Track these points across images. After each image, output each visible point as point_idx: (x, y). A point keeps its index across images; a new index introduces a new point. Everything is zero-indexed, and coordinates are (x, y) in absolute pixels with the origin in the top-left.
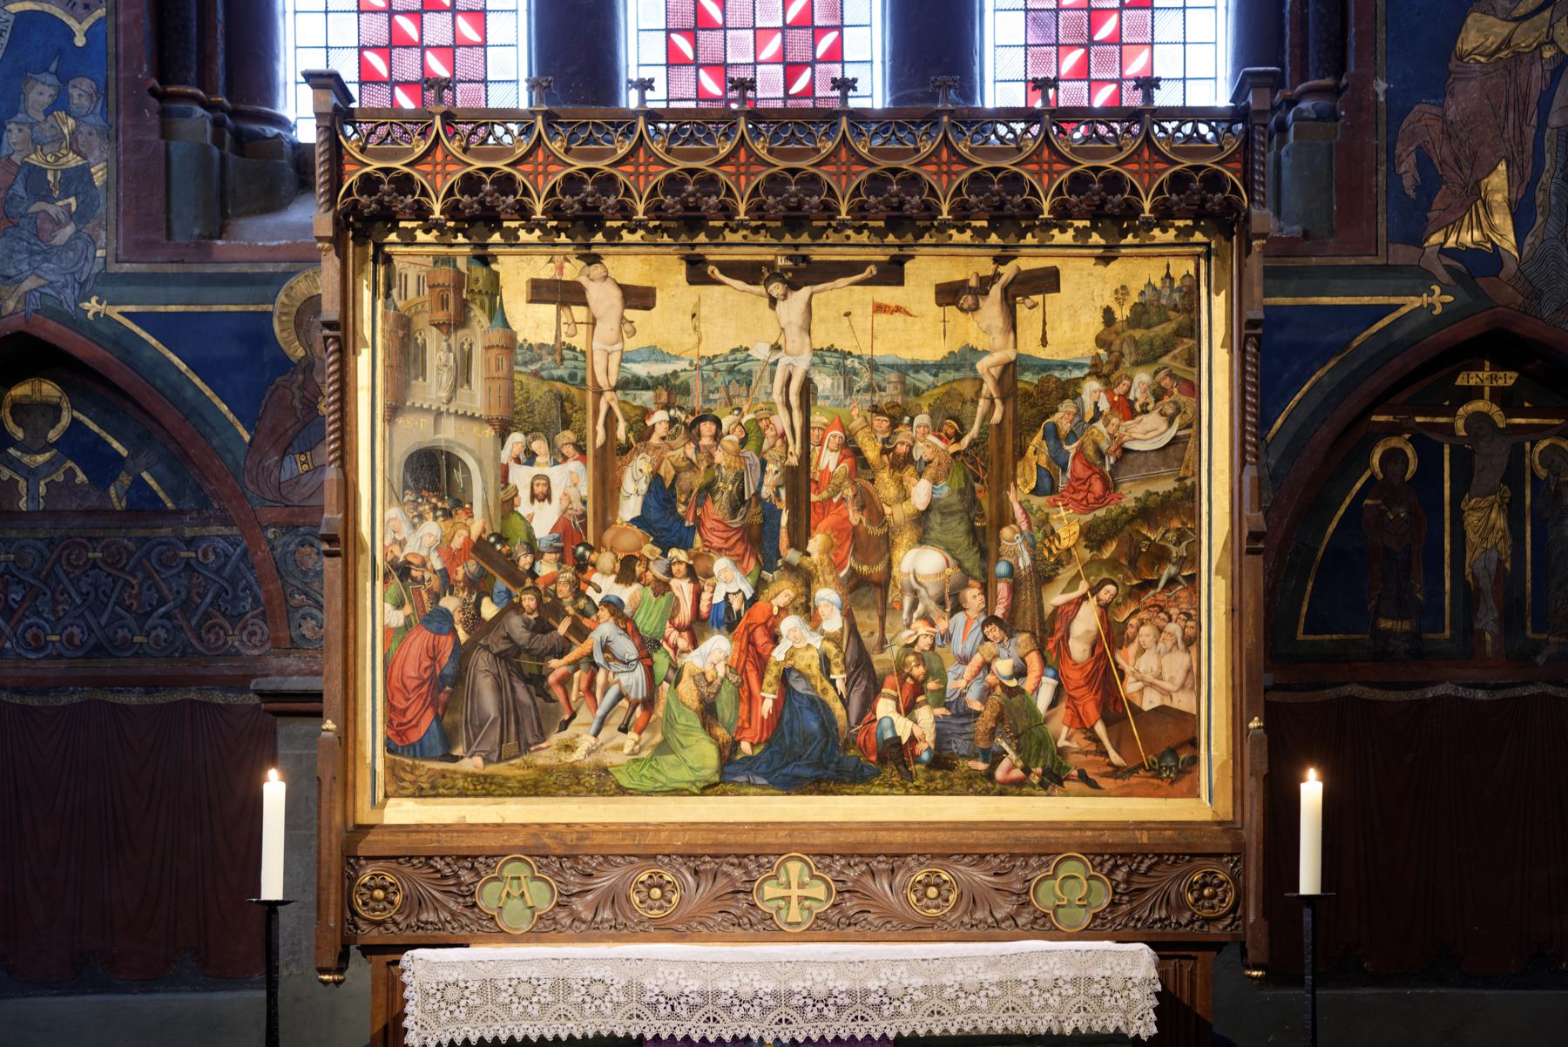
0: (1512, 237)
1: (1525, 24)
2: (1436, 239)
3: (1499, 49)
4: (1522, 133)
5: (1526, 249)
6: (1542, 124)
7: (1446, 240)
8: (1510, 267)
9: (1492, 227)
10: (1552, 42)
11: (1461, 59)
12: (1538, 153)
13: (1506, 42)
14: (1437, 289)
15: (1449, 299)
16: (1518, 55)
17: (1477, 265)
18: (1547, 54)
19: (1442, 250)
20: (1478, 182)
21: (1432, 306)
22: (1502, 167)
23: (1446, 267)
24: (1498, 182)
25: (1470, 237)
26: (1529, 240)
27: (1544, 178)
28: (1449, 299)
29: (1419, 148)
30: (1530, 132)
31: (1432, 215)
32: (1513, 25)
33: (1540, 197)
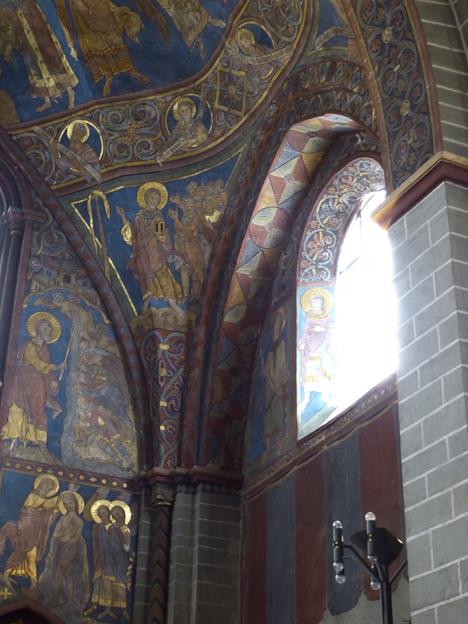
0: (35, 574)
1: (49, 500)
2: (9, 571)
3: (39, 507)
4: (43, 537)
5: (40, 580)
6: (51, 535)
7: (12, 571)
8: (34, 585)
9: (29, 570)
10: (58, 508)
11: (25, 508)
12: (48, 546)
13: (42, 506)
14: (6, 590)
15: (10, 594)
16: (45, 510)
17: (22, 583)
18: (55, 512)
19: (10, 576)
20: (26, 553)
21: (4, 596)
22: (35, 549)
23: (11, 582)
24: (33, 552)
25: (20, 572)
26: (42, 576)
27: (49, 555)
28: (10, 594)
29: (7, 537)
30: (46, 538)
31: (8, 562)
32: (44, 500)
33: (47, 561)
